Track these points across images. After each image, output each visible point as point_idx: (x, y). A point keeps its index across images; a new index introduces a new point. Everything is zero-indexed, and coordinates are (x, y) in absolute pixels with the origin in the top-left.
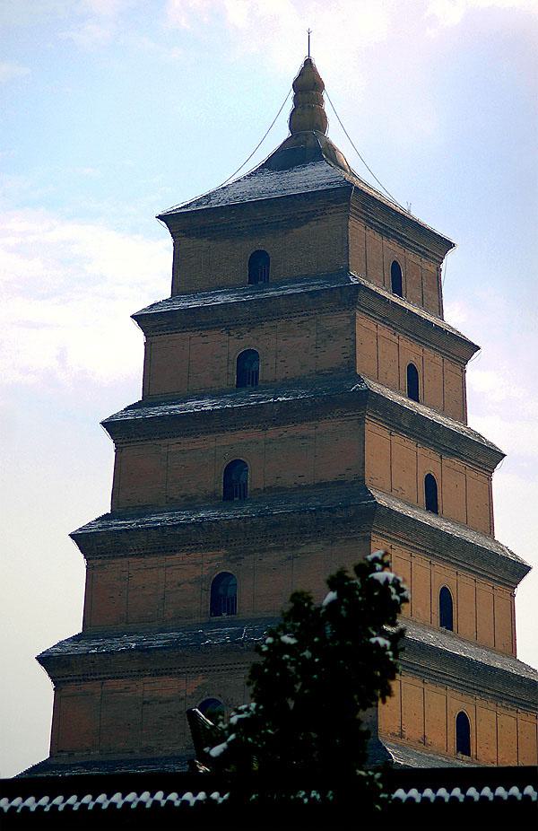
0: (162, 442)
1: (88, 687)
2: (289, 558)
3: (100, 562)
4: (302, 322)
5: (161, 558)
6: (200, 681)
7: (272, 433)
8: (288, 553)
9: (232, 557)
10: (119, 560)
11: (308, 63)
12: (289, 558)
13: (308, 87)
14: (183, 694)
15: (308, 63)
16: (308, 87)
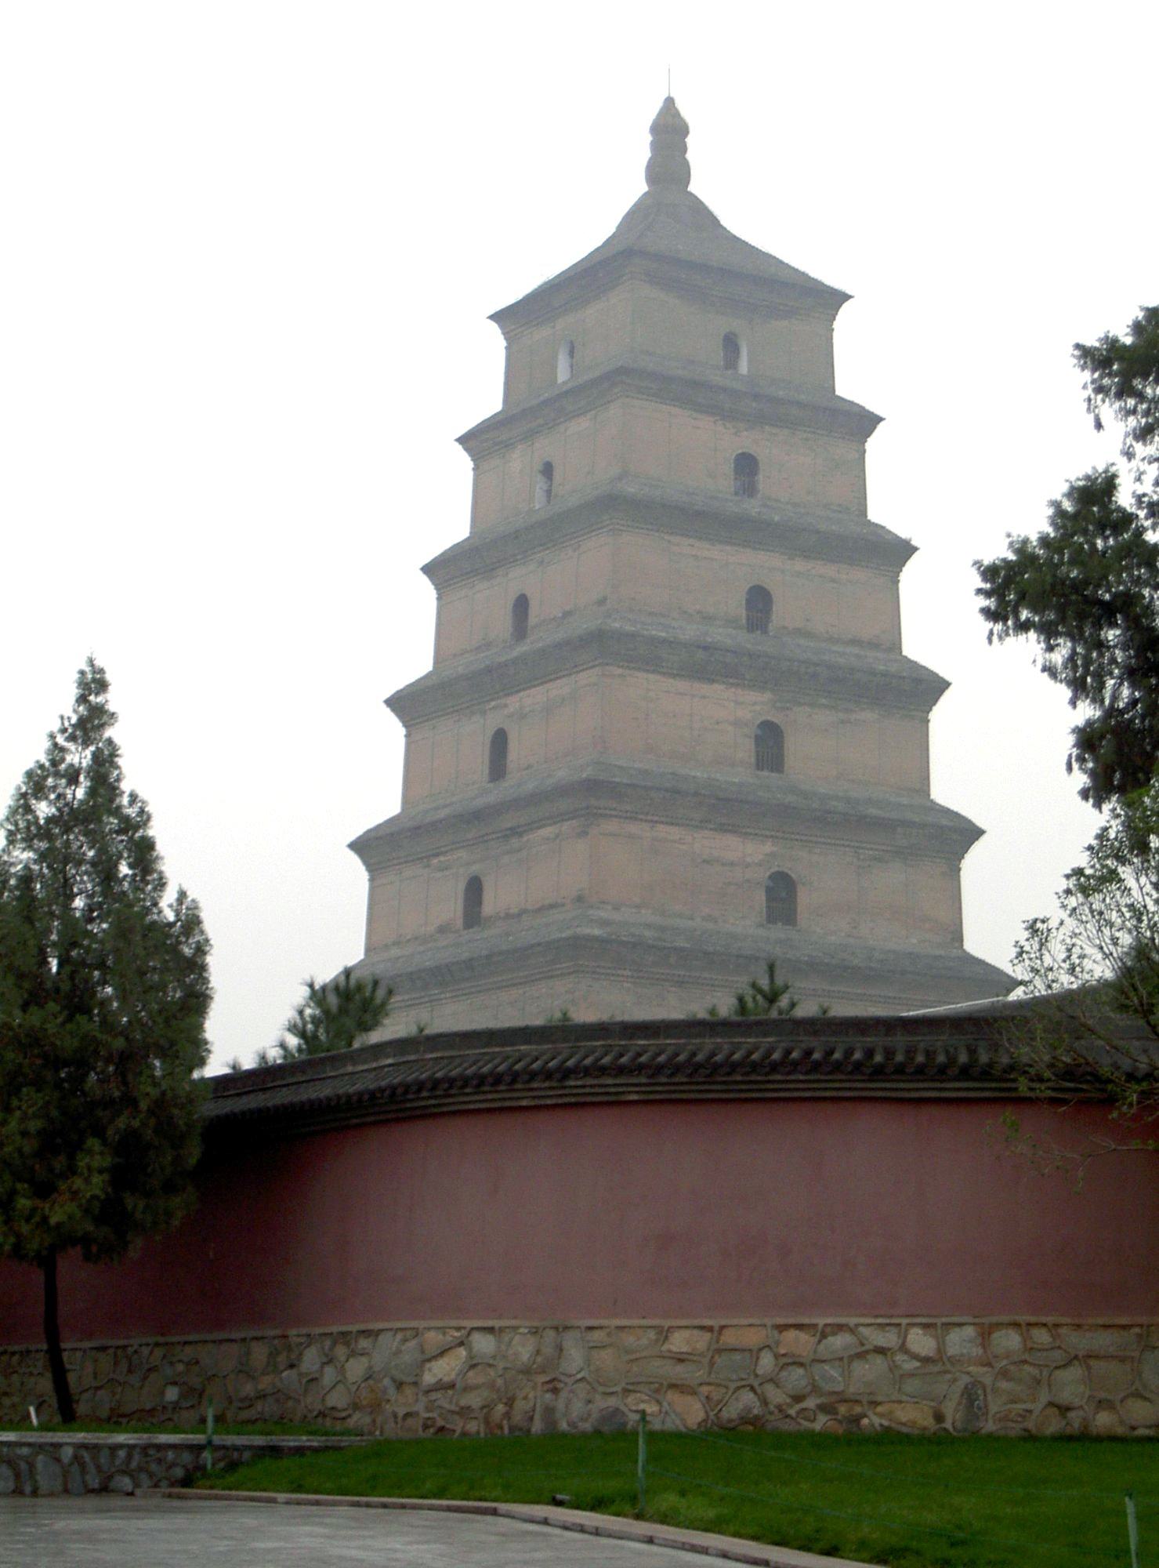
0: (672, 538)
1: (633, 828)
2: (843, 722)
3: (620, 671)
4: (807, 439)
5: (697, 685)
6: (768, 847)
7: (800, 565)
8: (841, 715)
9: (778, 705)
10: (645, 675)
11: (669, 102)
12: (843, 722)
13: (670, 133)
14: (748, 860)
15: (669, 102)
16: (670, 133)
